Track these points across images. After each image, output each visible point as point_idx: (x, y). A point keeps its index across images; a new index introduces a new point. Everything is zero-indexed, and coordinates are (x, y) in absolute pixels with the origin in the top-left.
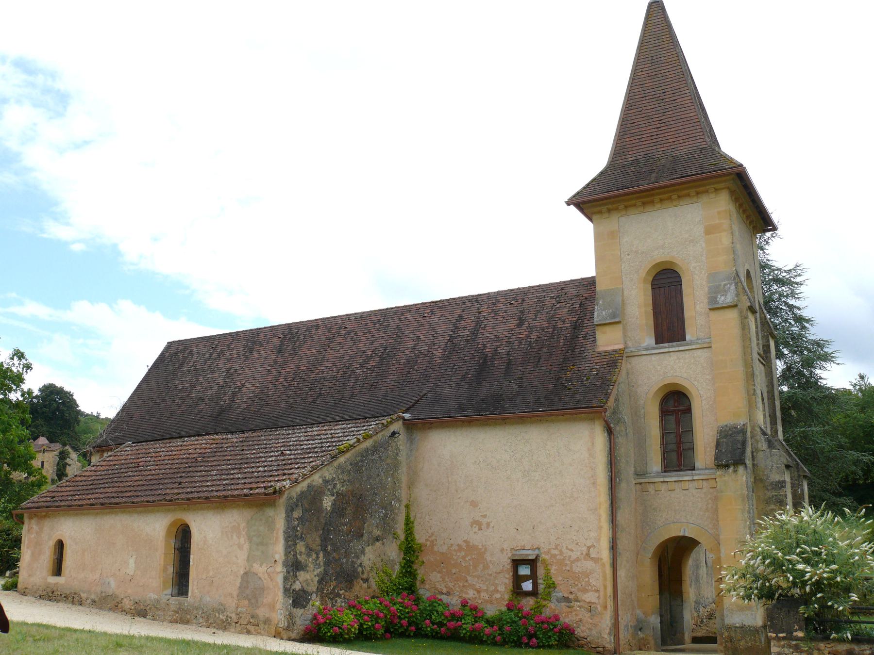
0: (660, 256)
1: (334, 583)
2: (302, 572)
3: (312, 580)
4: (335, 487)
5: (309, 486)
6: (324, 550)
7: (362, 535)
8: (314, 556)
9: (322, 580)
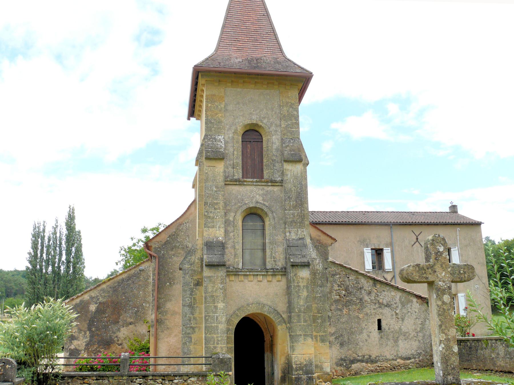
0: (255, 119)
1: (97, 346)
2: (75, 341)
3: (82, 344)
4: (98, 299)
5: (80, 301)
6: (90, 329)
7: (118, 322)
8: (83, 333)
9: (88, 345)
